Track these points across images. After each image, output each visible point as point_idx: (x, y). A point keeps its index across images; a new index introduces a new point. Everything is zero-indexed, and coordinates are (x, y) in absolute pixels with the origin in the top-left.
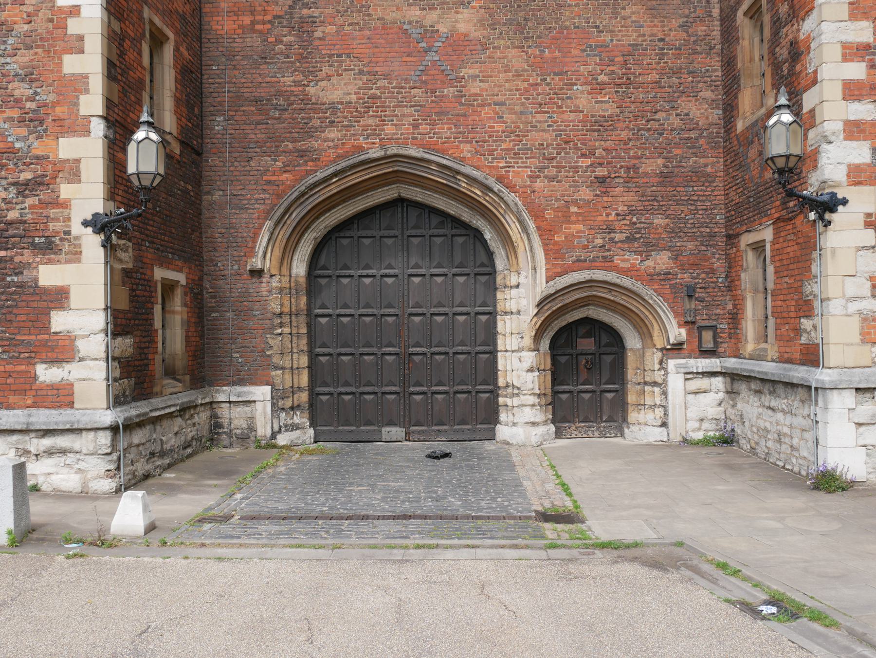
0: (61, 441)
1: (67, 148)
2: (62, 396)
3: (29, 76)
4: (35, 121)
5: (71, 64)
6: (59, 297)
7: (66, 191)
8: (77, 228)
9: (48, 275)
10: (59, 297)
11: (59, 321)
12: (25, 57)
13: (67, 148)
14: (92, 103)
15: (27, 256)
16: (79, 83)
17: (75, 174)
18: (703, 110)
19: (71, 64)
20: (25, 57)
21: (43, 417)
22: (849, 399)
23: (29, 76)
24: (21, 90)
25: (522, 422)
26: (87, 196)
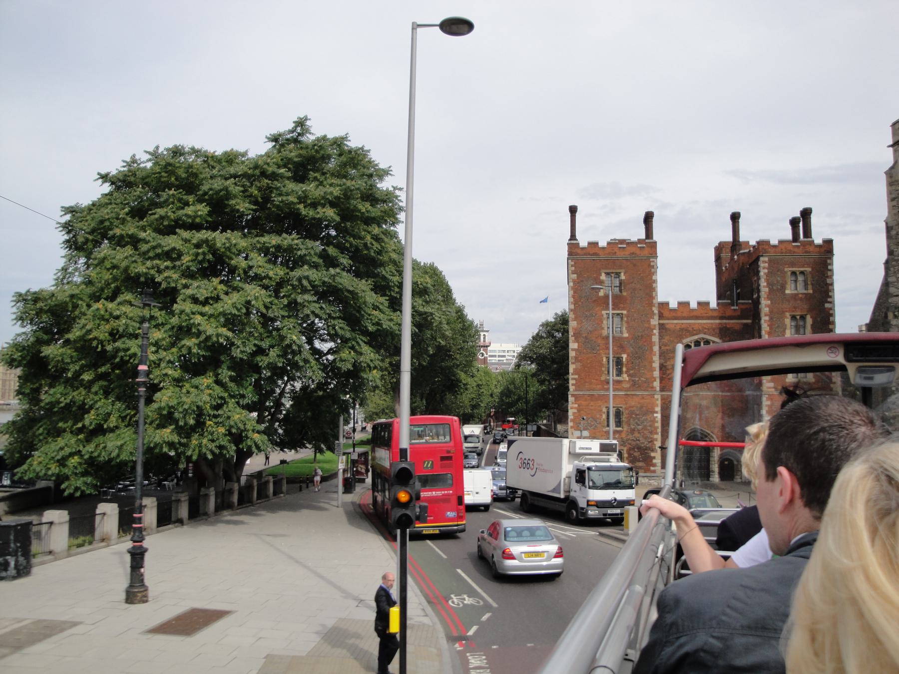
1: (655, 436)
2: (654, 472)
3: (650, 426)
4: (651, 433)
5: (656, 425)
6: (654, 458)
9: (653, 454)
10: (654, 458)
11: (654, 461)
13: (655, 436)
14: (659, 430)
16: (657, 428)
17: (656, 440)
19: (656, 425)
21: (653, 474)
23: (650, 426)
25: (715, 478)
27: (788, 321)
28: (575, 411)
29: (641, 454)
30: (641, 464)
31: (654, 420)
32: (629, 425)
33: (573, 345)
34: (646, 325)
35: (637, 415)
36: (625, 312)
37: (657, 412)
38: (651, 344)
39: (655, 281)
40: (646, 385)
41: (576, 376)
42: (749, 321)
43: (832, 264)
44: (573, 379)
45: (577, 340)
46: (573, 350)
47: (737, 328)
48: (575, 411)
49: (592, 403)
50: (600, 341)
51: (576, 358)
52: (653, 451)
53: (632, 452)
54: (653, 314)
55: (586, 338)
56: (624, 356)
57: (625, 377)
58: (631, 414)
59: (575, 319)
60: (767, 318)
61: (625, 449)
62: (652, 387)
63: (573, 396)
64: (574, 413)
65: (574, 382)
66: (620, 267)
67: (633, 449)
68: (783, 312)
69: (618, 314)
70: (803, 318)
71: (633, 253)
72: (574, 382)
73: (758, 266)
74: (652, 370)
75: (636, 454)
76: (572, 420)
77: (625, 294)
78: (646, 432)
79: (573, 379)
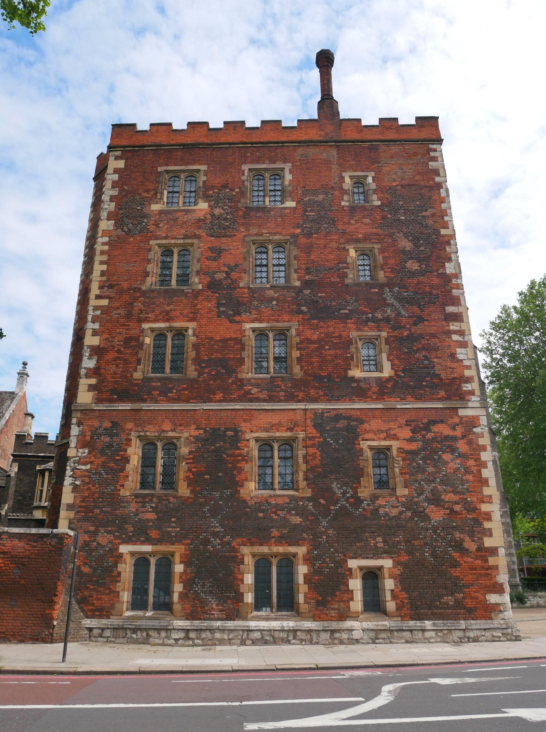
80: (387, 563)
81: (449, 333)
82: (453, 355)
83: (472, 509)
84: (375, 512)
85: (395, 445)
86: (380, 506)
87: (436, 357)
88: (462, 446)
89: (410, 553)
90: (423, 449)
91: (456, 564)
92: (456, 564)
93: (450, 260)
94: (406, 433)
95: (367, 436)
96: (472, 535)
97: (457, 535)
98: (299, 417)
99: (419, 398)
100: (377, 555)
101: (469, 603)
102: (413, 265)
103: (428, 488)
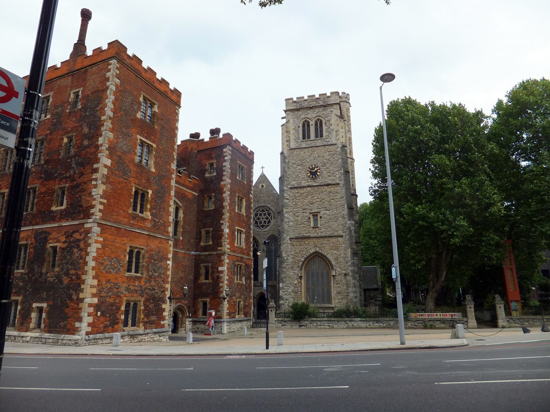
0: (164, 334)
2: (163, 326)
3: (163, 274)
7: (166, 292)
8: (167, 299)
9: (164, 306)
10: (164, 310)
11: (164, 314)
12: (163, 271)
14: (170, 279)
15: (161, 303)
18: (192, 277)
20: (163, 271)
22: (225, 323)
24: (163, 276)
26: (168, 294)
27: (237, 198)
28: (100, 246)
29: (155, 306)
30: (153, 318)
31: (167, 269)
32: (148, 271)
33: (105, 160)
34: (168, 167)
35: (155, 260)
36: (155, 146)
37: (169, 259)
38: (169, 187)
39: (177, 128)
40: (163, 227)
41: (105, 201)
42: (196, 194)
43: (252, 168)
44: (101, 203)
45: (110, 156)
46: (106, 166)
47: (190, 196)
48: (100, 246)
49: (118, 239)
50: (132, 167)
51: (107, 177)
52: (164, 302)
53: (148, 304)
54: (174, 159)
55: (120, 157)
56: (150, 192)
57: (147, 215)
58: (151, 257)
59: (112, 130)
60: (229, 193)
61: (143, 299)
62: (168, 232)
63: (99, 225)
64: (98, 249)
65: (101, 207)
66: (156, 99)
67: (150, 299)
68: (235, 192)
69: (149, 146)
70: (241, 200)
71: (166, 92)
72: (101, 207)
73: (222, 152)
74: (169, 214)
75: (151, 306)
76: (94, 259)
77: (156, 127)
78: (160, 280)
79: (101, 203)
80: (45, 305)
81: (91, 180)
82: (90, 194)
83: (79, 278)
84: (46, 280)
85: (58, 245)
86: (49, 277)
87: (84, 195)
88: (82, 245)
89: (53, 301)
90: (68, 247)
91: (67, 307)
92: (67, 307)
93: (101, 135)
94: (63, 239)
95: (50, 241)
96: (76, 292)
97: (71, 291)
98: (30, 233)
99: (73, 219)
100: (42, 302)
101: (69, 326)
102: (86, 142)
103: (65, 267)
